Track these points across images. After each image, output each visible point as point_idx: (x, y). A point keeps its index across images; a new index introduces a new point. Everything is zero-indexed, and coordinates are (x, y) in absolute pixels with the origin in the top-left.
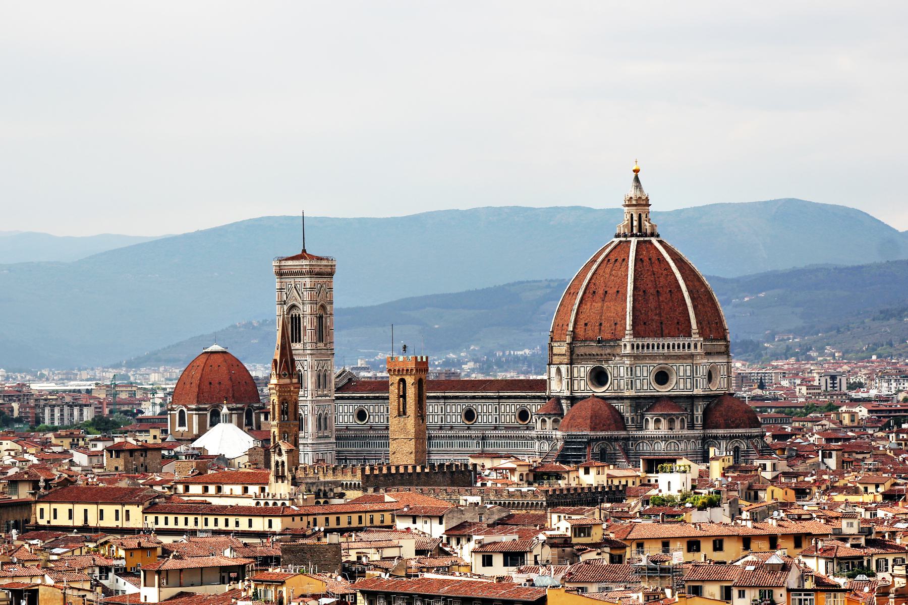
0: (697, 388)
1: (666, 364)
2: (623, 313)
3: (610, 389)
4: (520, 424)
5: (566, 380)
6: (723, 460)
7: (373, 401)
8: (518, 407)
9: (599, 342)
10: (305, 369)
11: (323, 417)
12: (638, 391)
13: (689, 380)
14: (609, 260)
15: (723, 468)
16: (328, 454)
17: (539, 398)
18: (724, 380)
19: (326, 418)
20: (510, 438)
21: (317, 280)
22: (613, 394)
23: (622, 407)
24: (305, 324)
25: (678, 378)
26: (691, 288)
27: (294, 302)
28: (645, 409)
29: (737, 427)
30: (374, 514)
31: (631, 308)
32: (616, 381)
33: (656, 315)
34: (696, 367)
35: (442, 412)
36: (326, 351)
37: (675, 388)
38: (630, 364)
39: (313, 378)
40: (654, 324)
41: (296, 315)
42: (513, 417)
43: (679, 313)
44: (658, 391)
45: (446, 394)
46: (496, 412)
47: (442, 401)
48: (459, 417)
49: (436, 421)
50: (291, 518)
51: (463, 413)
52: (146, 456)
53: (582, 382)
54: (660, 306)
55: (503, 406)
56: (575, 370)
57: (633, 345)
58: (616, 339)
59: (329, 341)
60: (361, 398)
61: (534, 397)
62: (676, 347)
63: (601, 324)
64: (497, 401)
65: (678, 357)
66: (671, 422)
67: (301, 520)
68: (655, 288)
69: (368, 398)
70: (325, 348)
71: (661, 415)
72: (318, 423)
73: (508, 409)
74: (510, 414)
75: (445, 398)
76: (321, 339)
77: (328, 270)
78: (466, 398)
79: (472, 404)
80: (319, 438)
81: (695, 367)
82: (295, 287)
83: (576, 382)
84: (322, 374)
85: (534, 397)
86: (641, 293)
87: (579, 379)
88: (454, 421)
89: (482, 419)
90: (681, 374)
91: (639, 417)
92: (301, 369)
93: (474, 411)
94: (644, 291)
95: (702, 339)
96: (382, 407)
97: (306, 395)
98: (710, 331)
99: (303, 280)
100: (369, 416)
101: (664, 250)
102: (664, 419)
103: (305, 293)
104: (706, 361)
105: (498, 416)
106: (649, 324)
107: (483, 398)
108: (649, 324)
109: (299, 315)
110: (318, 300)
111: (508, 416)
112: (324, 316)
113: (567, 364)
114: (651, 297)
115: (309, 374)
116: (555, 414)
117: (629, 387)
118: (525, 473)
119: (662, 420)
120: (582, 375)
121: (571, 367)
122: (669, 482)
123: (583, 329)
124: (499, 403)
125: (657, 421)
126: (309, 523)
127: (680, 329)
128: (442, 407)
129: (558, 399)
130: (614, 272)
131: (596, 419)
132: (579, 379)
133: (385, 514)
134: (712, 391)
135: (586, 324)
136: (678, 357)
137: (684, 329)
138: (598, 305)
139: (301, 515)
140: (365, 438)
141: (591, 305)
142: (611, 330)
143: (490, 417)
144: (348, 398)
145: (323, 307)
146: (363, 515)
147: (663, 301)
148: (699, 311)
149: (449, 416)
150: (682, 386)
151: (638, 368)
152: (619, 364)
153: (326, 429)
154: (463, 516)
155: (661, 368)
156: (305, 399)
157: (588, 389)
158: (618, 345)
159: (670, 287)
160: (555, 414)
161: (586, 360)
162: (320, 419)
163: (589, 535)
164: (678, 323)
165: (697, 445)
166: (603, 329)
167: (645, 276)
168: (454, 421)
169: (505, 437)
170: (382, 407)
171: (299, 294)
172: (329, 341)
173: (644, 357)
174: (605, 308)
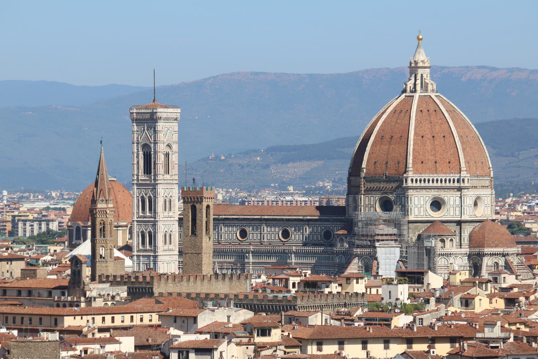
0: (464, 214)
4: (325, 242)
6: (460, 273)
8: (323, 228)
12: (416, 216)
13: (457, 209)
15: (460, 280)
16: (172, 264)
18: (487, 209)
19: (170, 235)
26: (461, 134)
29: (496, 246)
30: (144, 315)
33: (432, 155)
36: (172, 181)
37: (447, 214)
40: (430, 163)
42: (319, 236)
43: (451, 155)
44: (432, 217)
50: (73, 317)
52: (11, 264)
54: (435, 149)
67: (82, 318)
68: (432, 134)
70: (171, 179)
72: (164, 239)
73: (315, 229)
74: (317, 233)
79: (287, 225)
85: (336, 220)
86: (420, 138)
87: (370, 206)
88: (273, 238)
90: (452, 203)
94: (422, 137)
95: (469, 175)
98: (476, 169)
101: (440, 103)
104: (472, 193)
106: (426, 163)
108: (426, 163)
111: (315, 235)
114: (428, 142)
118: (297, 282)
122: (390, 292)
123: (373, 166)
126: (88, 321)
127: (451, 167)
130: (399, 121)
133: (153, 314)
134: (477, 217)
137: (454, 167)
138: (385, 147)
139: (82, 315)
146: (134, 315)
147: (437, 145)
148: (467, 153)
149: (269, 235)
150: (452, 213)
151: (416, 198)
152: (401, 194)
154: (214, 317)
155: (435, 198)
159: (443, 134)
162: (165, 236)
163: (269, 335)
164: (449, 162)
165: (464, 261)
167: (424, 124)
168: (273, 238)
174: (391, 150)
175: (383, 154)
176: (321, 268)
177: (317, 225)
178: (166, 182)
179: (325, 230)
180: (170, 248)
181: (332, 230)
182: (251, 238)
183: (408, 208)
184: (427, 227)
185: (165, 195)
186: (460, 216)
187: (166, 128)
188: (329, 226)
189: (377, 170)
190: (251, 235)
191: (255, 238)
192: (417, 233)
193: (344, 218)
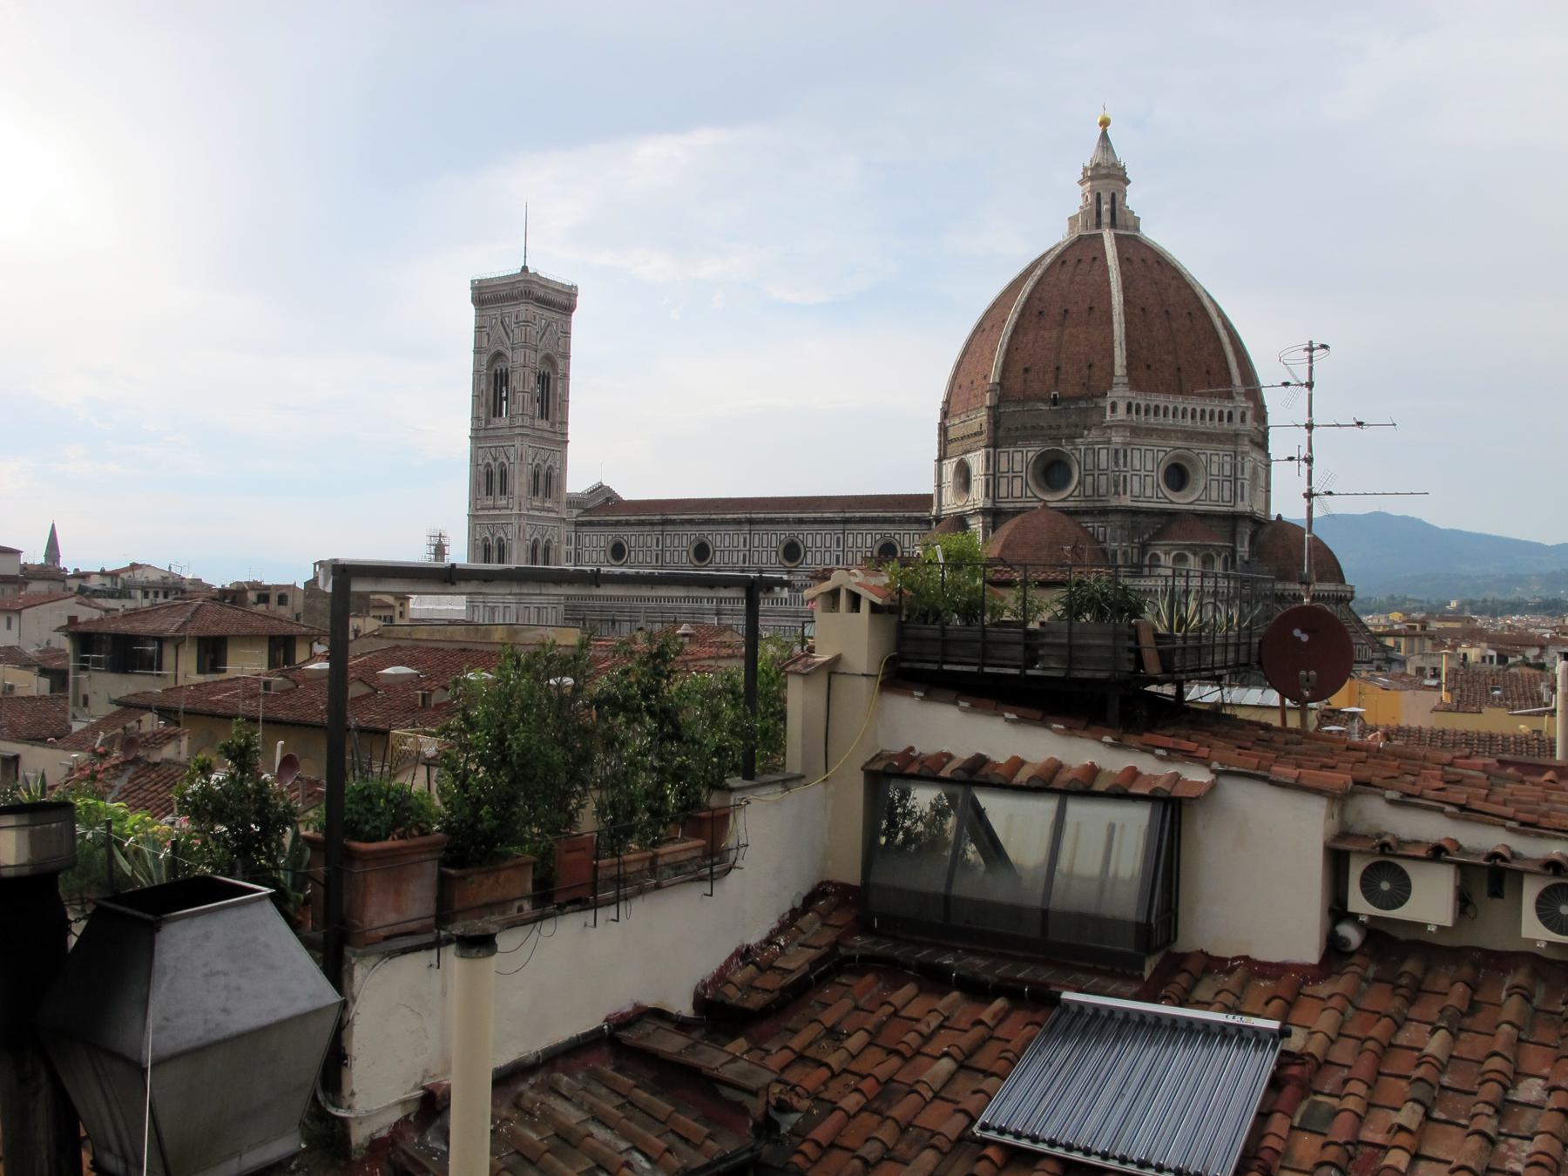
1: (1188, 449)
3: (1076, 493)
7: (636, 528)
8: (878, 537)
9: (1055, 401)
10: (512, 461)
11: (541, 545)
12: (1135, 498)
14: (1064, 262)
16: (550, 610)
17: (918, 521)
21: (540, 311)
22: (1083, 504)
23: (1101, 529)
24: (514, 384)
25: (1209, 478)
27: (500, 348)
31: (1123, 336)
32: (1089, 479)
35: (745, 546)
36: (552, 435)
37: (1203, 497)
38: (1124, 444)
41: (501, 370)
44: (1172, 502)
46: (838, 546)
47: (746, 527)
49: (735, 560)
51: (782, 547)
53: (1017, 482)
55: (850, 536)
56: (1004, 459)
58: (1093, 392)
60: (617, 523)
61: (909, 521)
63: (1058, 368)
65: (1210, 437)
66: (1207, 560)
69: (628, 523)
73: (859, 540)
75: (751, 522)
77: (562, 299)
78: (786, 521)
82: (502, 322)
83: (1004, 482)
84: (543, 472)
85: (909, 521)
86: (1138, 311)
87: (1010, 474)
89: (814, 557)
90: (1215, 471)
91: (1135, 551)
92: (505, 460)
93: (800, 543)
94: (1143, 309)
97: (511, 506)
100: (630, 551)
102: (1195, 554)
103: (516, 331)
105: (841, 554)
107: (815, 521)
109: (507, 370)
112: (552, 376)
115: (517, 468)
117: (1121, 489)
119: (1191, 557)
120: (1017, 468)
121: (995, 451)
124: (844, 530)
125: (1181, 558)
128: (745, 539)
130: (1078, 279)
132: (1010, 474)
136: (1210, 437)
144: (599, 524)
145: (549, 359)
149: (756, 553)
150: (1214, 495)
151: (1136, 453)
152: (1098, 443)
155: (1177, 456)
156: (508, 512)
157: (1029, 494)
158: (1097, 406)
161: (1026, 438)
164: (1208, 372)
166: (1062, 376)
170: (649, 538)
172: (558, 419)
173: (1150, 431)
177: (864, 532)
178: (539, 433)
179: (881, 543)
183: (1119, 476)
184: (1159, 526)
185: (536, 462)
186: (1232, 504)
187: (544, 321)
188: (893, 532)
190: (718, 554)
191: (726, 560)
193: (927, 514)
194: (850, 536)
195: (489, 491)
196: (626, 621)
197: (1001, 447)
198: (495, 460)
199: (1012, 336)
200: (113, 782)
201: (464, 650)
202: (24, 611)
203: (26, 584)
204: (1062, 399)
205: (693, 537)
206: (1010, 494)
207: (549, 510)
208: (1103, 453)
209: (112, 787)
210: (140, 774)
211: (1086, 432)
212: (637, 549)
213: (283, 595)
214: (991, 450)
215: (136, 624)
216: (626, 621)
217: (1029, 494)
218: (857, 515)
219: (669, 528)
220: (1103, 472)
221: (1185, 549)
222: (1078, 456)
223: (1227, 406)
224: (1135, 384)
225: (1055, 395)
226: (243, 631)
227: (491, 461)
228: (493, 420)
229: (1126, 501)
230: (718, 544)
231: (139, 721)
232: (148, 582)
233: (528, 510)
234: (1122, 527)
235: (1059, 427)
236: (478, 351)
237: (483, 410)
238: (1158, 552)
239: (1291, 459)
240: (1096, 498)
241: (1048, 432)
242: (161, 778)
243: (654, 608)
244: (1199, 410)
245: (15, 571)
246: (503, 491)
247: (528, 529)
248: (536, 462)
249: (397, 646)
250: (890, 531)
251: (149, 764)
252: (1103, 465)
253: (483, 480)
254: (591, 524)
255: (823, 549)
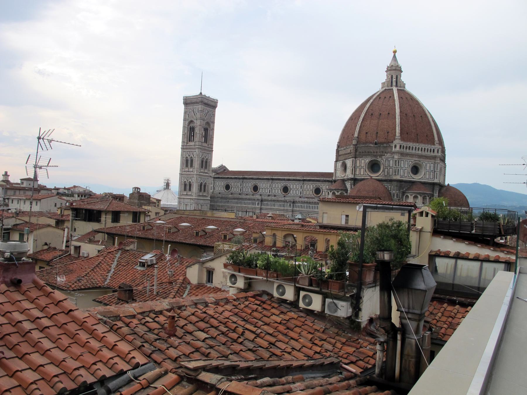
0: (437, 178)
1: (419, 161)
2: (393, 126)
3: (382, 174)
4: (315, 196)
5: (351, 168)
7: (234, 180)
8: (314, 186)
9: (376, 144)
10: (195, 156)
11: (203, 184)
12: (401, 176)
14: (380, 98)
16: (205, 206)
17: (328, 181)
19: (205, 186)
20: (310, 203)
21: (206, 108)
22: (384, 178)
24: (196, 131)
25: (426, 171)
27: (192, 119)
28: (404, 189)
31: (399, 123)
32: (386, 170)
34: (437, 165)
35: (270, 187)
38: (398, 159)
39: (198, 161)
41: (192, 126)
44: (413, 178)
45: (273, 177)
46: (301, 188)
47: (271, 181)
48: (279, 190)
49: (266, 192)
51: (282, 188)
53: (362, 170)
55: (305, 185)
56: (358, 162)
57: (401, 146)
59: (210, 143)
60: (228, 178)
61: (325, 181)
62: (426, 151)
63: (377, 133)
64: (302, 182)
65: (426, 157)
69: (231, 178)
71: (419, 193)
72: (199, 188)
73: (308, 187)
75: (272, 179)
76: (206, 141)
78: (284, 180)
80: (199, 196)
81: (436, 165)
83: (358, 169)
84: (204, 160)
85: (325, 181)
86: (404, 115)
88: (276, 192)
90: (428, 169)
91: (401, 194)
92: (192, 156)
93: (288, 187)
94: (406, 114)
96: (238, 183)
99: (198, 107)
102: (421, 196)
103: (198, 114)
105: (302, 191)
110: (205, 119)
113: (352, 158)
114: (411, 118)
116: (342, 190)
117: (397, 173)
119: (419, 197)
121: (355, 159)
124: (303, 183)
128: (270, 185)
129: (343, 181)
131: (376, 192)
132: (360, 167)
135: (367, 133)
136: (426, 157)
140: (226, 198)
141: (370, 122)
142: (385, 136)
143: (297, 191)
144: (222, 178)
145: (208, 123)
149: (274, 190)
150: (427, 177)
151: (402, 162)
152: (389, 158)
153: (205, 191)
155: (416, 163)
156: (193, 173)
157: (366, 174)
158: (390, 146)
160: (342, 190)
161: (366, 155)
166: (378, 135)
167: (406, 106)
168: (276, 192)
169: (307, 203)
170: (238, 183)
171: (195, 115)
172: (210, 143)
173: (407, 155)
174: (380, 123)
175: (373, 126)
176: (314, 215)
178: (204, 148)
179: (316, 188)
180: (204, 194)
181: (322, 188)
182: (261, 192)
183: (396, 169)
184: (409, 186)
185: (203, 157)
187: (207, 111)
188: (319, 185)
189: (368, 139)
190: (261, 189)
191: (264, 192)
192: (401, 191)
193: (331, 179)
194: (305, 185)
195: (187, 166)
196: (251, 212)
197: (357, 158)
198: (189, 156)
199: (362, 121)
200: (116, 255)
201: (204, 219)
202: (42, 200)
203: (40, 191)
204: (378, 143)
205: (253, 184)
206: (360, 173)
207: (206, 173)
208: (391, 161)
209: (116, 257)
210: (123, 253)
211: (386, 154)
212: (234, 187)
213: (120, 198)
214: (354, 159)
215: (92, 206)
216: (251, 212)
217: (366, 174)
218: (308, 178)
219: (245, 180)
220: (391, 168)
221: (417, 194)
222: (383, 162)
223: (433, 147)
224: (403, 139)
225: (376, 142)
226: (126, 210)
227: (188, 156)
228: (189, 143)
229: (398, 177)
230: (261, 186)
231: (94, 237)
232: (79, 192)
233: (199, 173)
234: (397, 186)
235: (377, 152)
236: (185, 120)
237: (186, 139)
238: (408, 195)
239: (525, 183)
240: (388, 176)
241: (373, 154)
242: (131, 254)
243: (240, 207)
244: (423, 148)
245: (36, 187)
246: (192, 166)
247: (199, 179)
248: (203, 157)
249: (181, 217)
250: (318, 184)
251: (125, 250)
252: (391, 165)
253: (185, 162)
254: (219, 178)
255: (296, 189)
